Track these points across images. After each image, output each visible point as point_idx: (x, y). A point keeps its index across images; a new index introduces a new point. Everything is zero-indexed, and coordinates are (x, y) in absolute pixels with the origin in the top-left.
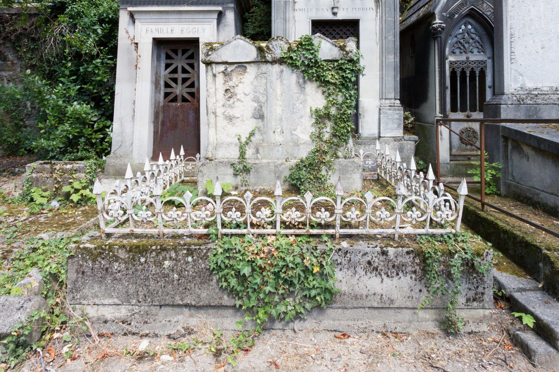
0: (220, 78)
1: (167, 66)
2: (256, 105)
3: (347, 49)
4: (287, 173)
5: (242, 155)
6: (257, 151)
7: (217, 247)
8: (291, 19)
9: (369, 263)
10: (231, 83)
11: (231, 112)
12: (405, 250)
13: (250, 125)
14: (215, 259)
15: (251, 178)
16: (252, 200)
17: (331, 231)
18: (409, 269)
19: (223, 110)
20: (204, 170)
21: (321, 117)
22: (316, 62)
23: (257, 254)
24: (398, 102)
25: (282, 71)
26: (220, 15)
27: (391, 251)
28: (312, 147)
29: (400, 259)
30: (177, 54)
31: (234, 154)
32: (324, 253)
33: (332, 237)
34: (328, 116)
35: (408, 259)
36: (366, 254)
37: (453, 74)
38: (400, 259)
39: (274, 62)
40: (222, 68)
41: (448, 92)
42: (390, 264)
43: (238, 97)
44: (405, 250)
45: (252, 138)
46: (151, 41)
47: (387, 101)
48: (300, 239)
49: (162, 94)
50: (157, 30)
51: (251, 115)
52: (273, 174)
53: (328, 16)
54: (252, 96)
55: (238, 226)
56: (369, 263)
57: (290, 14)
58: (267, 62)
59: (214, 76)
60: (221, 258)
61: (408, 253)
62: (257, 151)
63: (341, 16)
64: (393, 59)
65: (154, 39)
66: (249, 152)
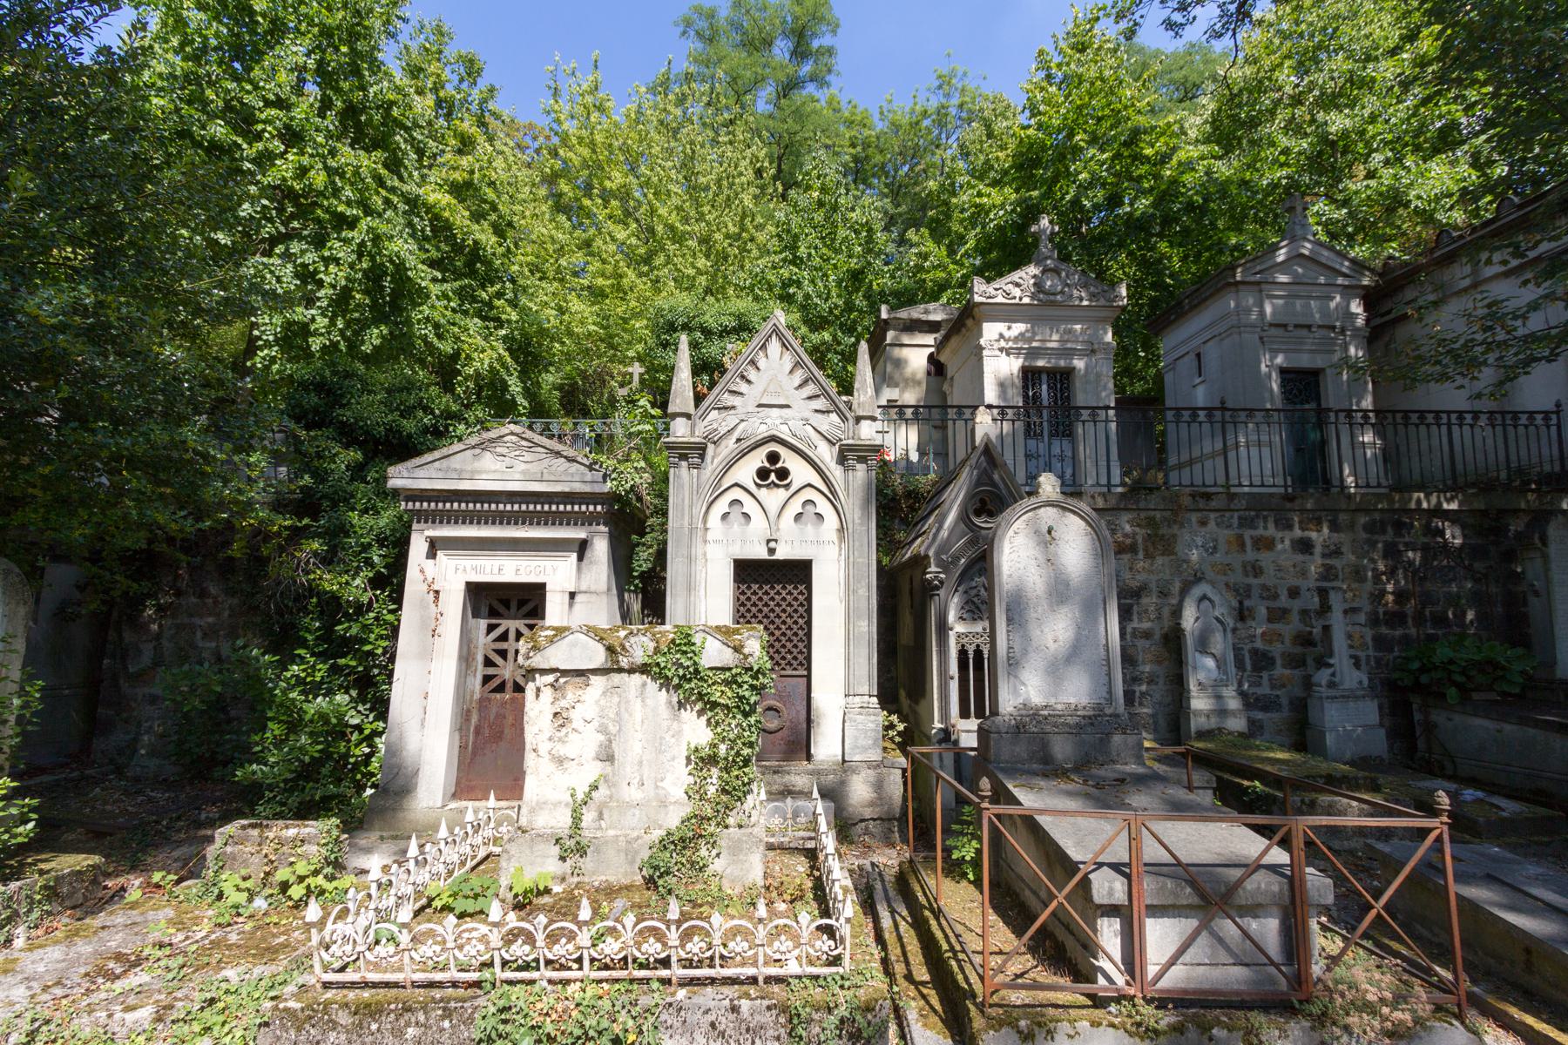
0: (547, 693)
1: (491, 628)
2: (602, 738)
3: (746, 651)
4: (645, 854)
5: (577, 820)
6: (601, 816)
7: (487, 1004)
8: (700, 557)
9: (713, 1025)
10: (563, 703)
11: (562, 750)
12: (766, 1003)
13: (593, 770)
14: (482, 1024)
15: (587, 863)
16: (546, 928)
17: (664, 973)
18: (771, 1033)
19: (549, 745)
20: (513, 848)
21: (704, 760)
22: (697, 671)
23: (547, 1014)
24: (875, 700)
25: (644, 685)
26: (582, 548)
27: (745, 1004)
28: (687, 810)
29: (757, 1017)
30: (508, 608)
31: (561, 821)
32: (648, 1011)
33: (666, 982)
34: (712, 760)
35: (768, 1018)
36: (707, 1012)
37: (963, 653)
38: (757, 1017)
39: (631, 671)
40: (550, 678)
41: (954, 687)
42: (744, 1026)
43: (574, 725)
44: (766, 1003)
45: (594, 794)
46: (462, 587)
47: (857, 699)
48: (617, 986)
49: (479, 678)
50: (475, 569)
51: (593, 754)
52: (623, 855)
53: (762, 554)
54: (595, 724)
55: (526, 967)
56: (713, 1025)
57: (698, 549)
58: (620, 670)
59: (538, 690)
60: (492, 1021)
61: (769, 1008)
62: (601, 816)
63: (782, 554)
64: (867, 627)
65: (468, 584)
66: (588, 817)
